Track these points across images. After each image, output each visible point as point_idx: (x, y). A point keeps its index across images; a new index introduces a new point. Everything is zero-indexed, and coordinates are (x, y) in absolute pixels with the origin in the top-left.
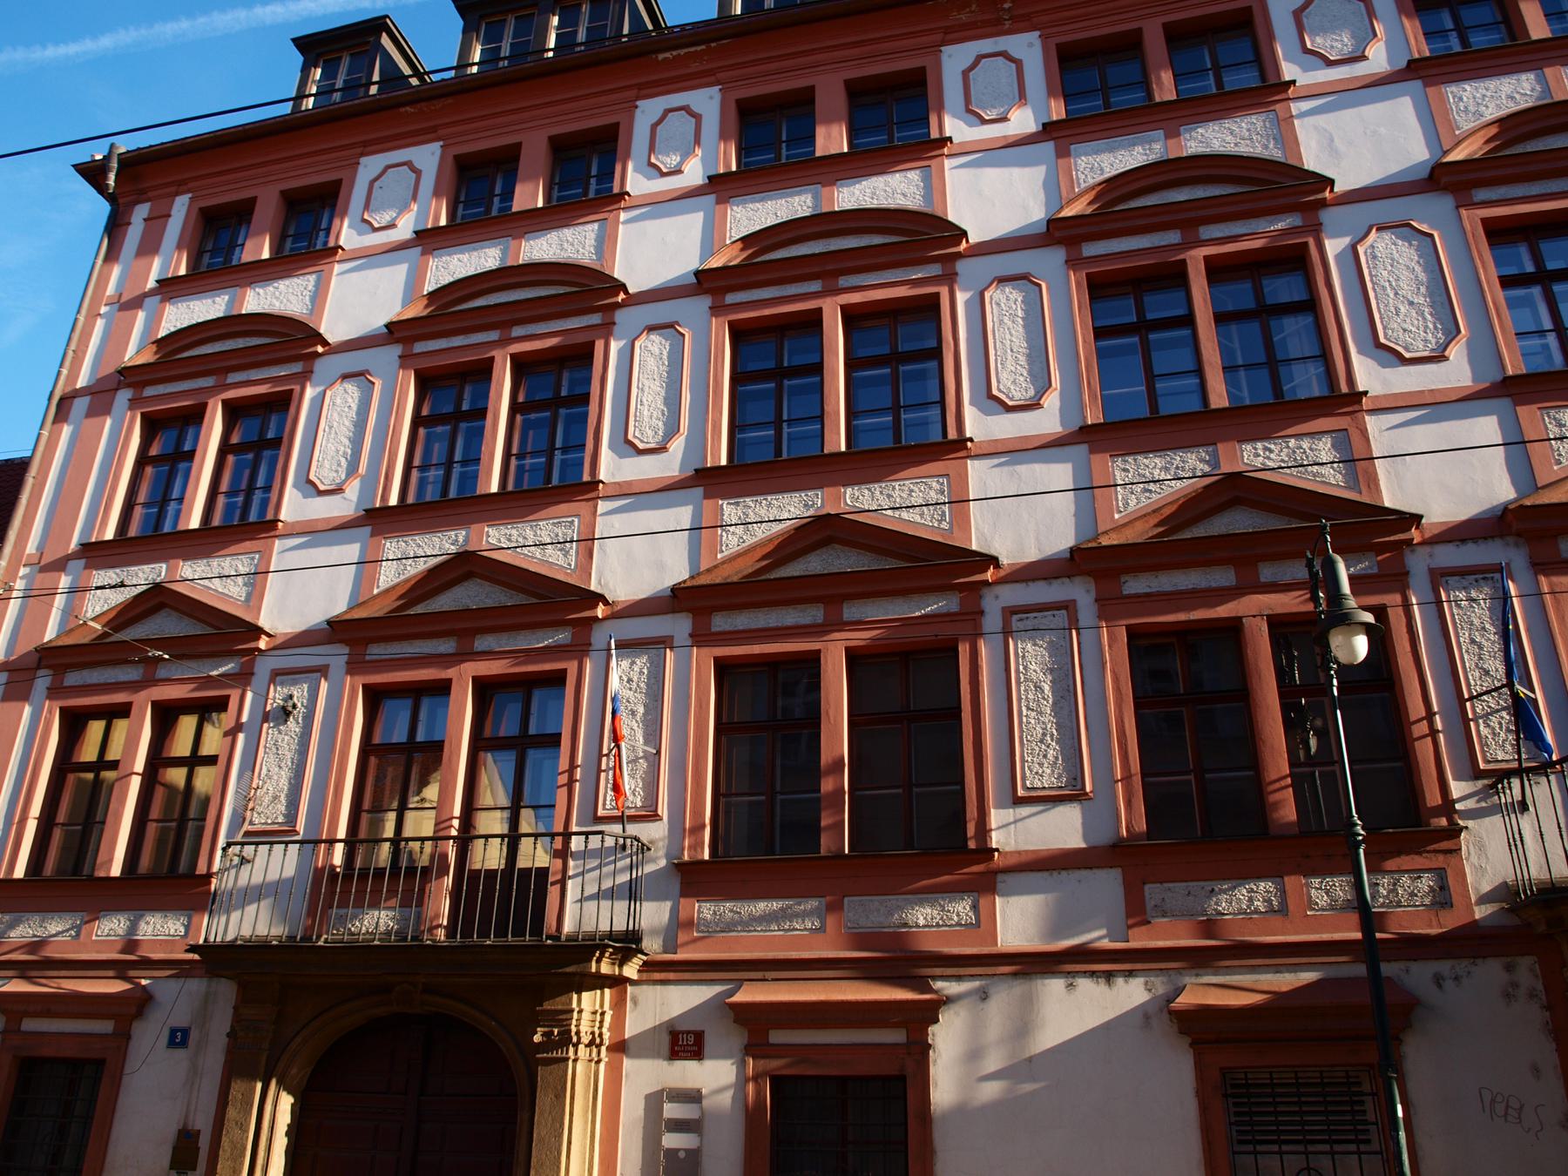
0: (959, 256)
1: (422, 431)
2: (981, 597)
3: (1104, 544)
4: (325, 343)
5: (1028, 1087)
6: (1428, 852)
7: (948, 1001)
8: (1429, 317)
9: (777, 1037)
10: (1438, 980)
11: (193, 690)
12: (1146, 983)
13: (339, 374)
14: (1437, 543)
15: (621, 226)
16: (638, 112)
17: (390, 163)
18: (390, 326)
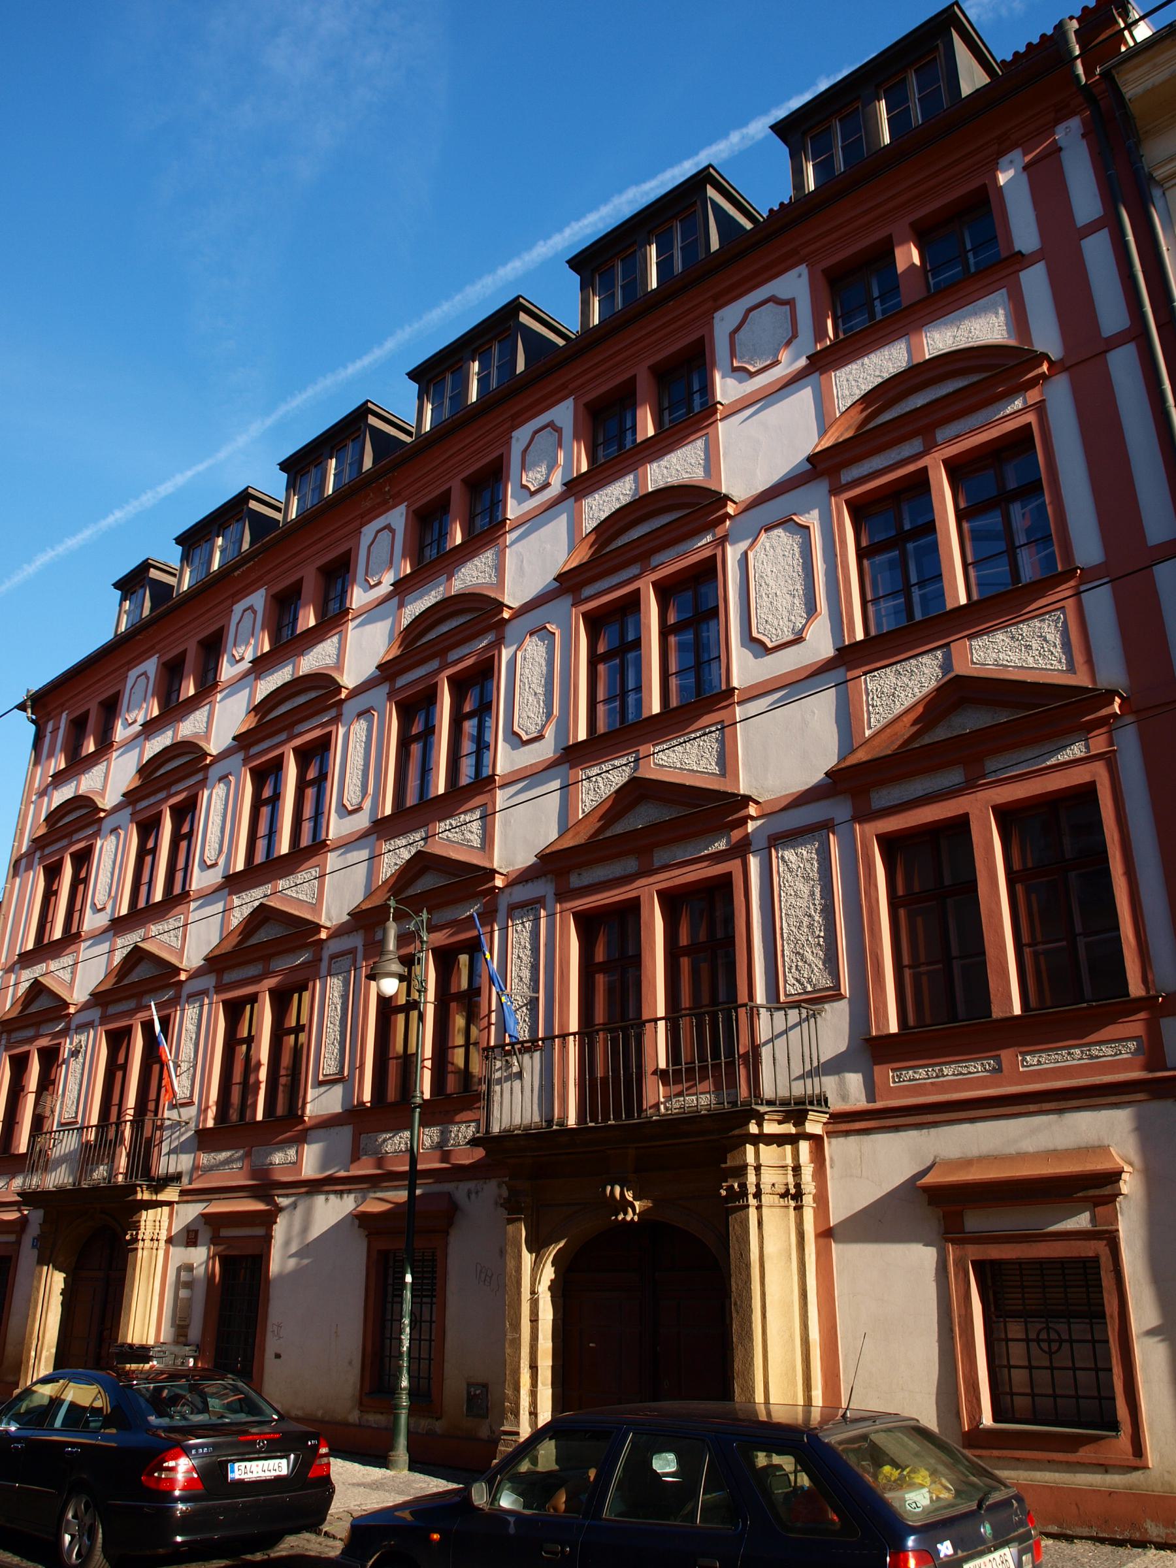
0: (208, 766)
1: (672, 640)
2: (322, 949)
3: (364, 908)
4: (104, 811)
5: (306, 1261)
6: (475, 1108)
7: (281, 1210)
8: (542, 703)
9: (224, 1232)
10: (469, 1193)
11: (50, 1041)
12: (355, 1197)
13: (355, 714)
14: (514, 884)
15: (217, 705)
16: (362, 535)
17: (378, 529)
18: (560, 578)
